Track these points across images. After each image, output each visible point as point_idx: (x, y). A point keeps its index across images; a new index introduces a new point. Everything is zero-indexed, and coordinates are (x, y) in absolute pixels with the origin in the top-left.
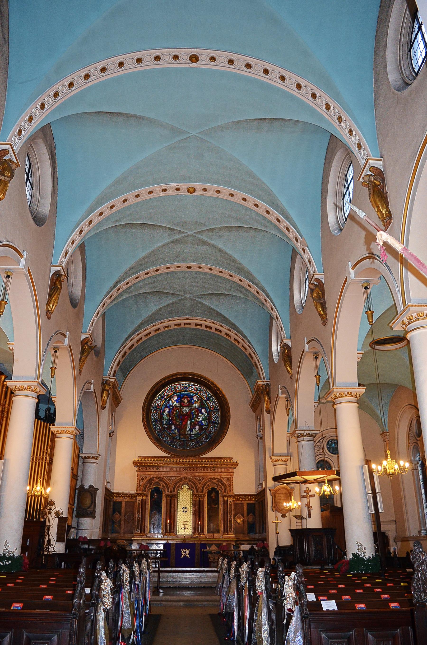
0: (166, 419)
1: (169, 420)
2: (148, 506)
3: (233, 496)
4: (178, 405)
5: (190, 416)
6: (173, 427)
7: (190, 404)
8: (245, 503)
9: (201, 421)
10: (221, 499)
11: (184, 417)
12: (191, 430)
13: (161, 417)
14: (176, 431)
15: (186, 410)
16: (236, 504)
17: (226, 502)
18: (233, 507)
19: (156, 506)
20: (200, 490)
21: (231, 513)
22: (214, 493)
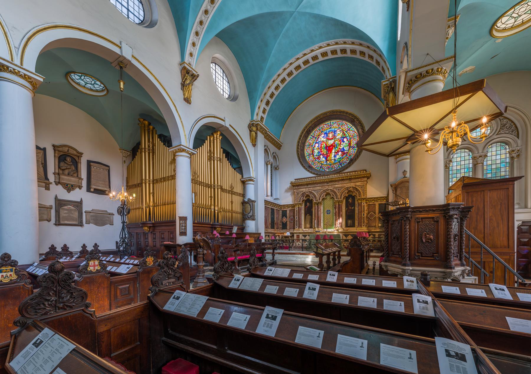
0: (316, 152)
1: (319, 152)
2: (303, 212)
3: (367, 200)
4: (324, 140)
5: (333, 146)
6: (322, 156)
7: (334, 137)
8: (377, 204)
9: (343, 148)
10: (356, 203)
11: (329, 149)
12: (335, 156)
13: (313, 151)
14: (324, 159)
15: (331, 142)
16: (369, 206)
17: (360, 205)
18: (366, 208)
19: (309, 211)
20: (339, 197)
21: (364, 211)
22: (351, 198)
